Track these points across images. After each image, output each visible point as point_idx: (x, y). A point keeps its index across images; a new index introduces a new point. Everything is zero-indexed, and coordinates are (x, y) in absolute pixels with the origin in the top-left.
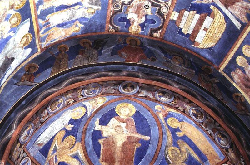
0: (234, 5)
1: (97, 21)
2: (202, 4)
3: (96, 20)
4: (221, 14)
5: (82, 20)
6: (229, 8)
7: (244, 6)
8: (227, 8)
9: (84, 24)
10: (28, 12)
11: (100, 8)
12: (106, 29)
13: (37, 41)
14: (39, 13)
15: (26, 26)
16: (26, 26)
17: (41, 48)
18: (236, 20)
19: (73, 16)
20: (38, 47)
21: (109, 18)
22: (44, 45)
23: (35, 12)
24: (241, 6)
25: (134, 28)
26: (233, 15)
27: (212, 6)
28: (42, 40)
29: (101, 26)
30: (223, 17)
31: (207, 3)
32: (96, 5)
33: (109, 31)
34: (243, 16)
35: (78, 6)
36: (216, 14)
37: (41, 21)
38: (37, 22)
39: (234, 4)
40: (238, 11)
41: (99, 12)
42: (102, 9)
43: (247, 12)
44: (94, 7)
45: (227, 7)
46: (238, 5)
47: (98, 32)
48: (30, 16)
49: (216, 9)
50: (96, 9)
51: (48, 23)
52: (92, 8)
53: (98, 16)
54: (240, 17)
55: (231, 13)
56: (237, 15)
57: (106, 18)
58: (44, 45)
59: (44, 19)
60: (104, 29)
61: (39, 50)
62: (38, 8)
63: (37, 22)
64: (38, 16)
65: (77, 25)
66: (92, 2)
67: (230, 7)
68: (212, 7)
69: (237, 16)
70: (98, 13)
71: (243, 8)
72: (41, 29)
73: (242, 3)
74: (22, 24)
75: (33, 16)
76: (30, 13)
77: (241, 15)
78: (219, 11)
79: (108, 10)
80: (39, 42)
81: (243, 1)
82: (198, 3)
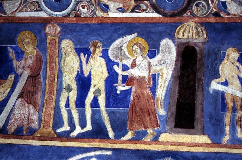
0: (27, 104)
2: (11, 61)
4: (6, 94)
6: (20, 100)
7: (31, 118)
8: (18, 98)
18: (6, 117)
24: (29, 114)
26: (12, 110)
27: (13, 76)
30: (4, 98)
31: (15, 67)
34: (17, 123)
36: (3, 87)
39: (28, 103)
40: (21, 113)
43: (25, 125)
45: (21, 96)
46: (29, 110)
49: (12, 84)
54: (13, 120)
55: (14, 106)
56: (14, 115)
67: (22, 101)
68: (12, 77)
69: (12, 115)
71: (28, 118)
73: (34, 113)
77: (16, 120)
78: (9, 89)
81: (37, 113)
82: (11, 55)
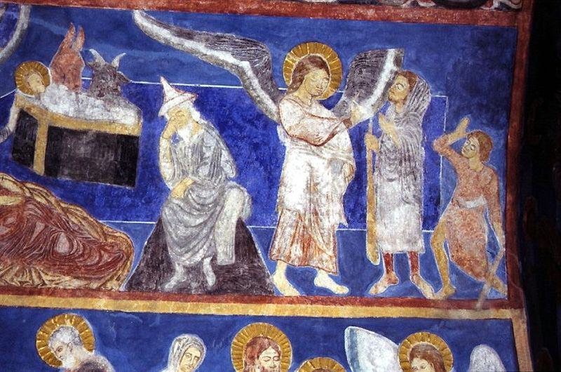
1: (455, 66)
3: (449, 67)
9: (456, 117)
10: (319, 328)
11: (392, 53)
12: (505, 23)
14: (341, 290)
17: (499, 304)
20: (492, 314)
21: (451, 12)
23: (334, 303)
29: (481, 44)
32: (376, 69)
33: (517, 11)
35: (370, 142)
37: (380, 287)
38: (379, 301)
41: (412, 54)
42: (392, 43)
44: (384, 77)
47: (513, 56)
48: (341, 324)
50: (395, 69)
51: (399, 262)
52: (389, 85)
53: (428, 60)
57: (447, 29)
58: (493, 286)
59: (377, 273)
60: (503, 28)
61: (507, 314)
62: (325, 291)
63: (379, 301)
64: (351, 294)
65: (457, 147)
66: (362, 84)
70: (416, 62)
72: (414, 289)
74: (355, 358)
75: (344, 312)
76: (327, 321)
79: (408, 20)
80: (469, 308)
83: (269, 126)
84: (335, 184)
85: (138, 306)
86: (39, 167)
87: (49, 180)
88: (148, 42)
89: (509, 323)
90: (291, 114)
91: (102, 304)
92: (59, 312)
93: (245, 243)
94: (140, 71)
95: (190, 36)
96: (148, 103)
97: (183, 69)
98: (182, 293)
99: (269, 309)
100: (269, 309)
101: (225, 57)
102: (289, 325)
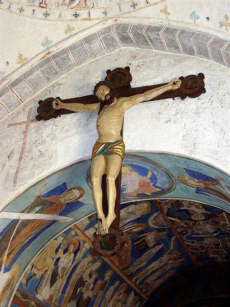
5: (172, 269)
13: (143, 295)
14: (138, 284)
15: (132, 294)
16: (132, 294)
19: (165, 271)
22: (149, 294)
25: (220, 260)
28: (144, 293)
51: (147, 283)
75: (134, 287)
83: (162, 255)
84: (156, 268)
85: (119, 272)
86: (135, 244)
87: (133, 246)
88: (170, 240)
89: (145, 299)
90: (165, 258)
91: (117, 270)
92: (112, 268)
93: (138, 270)
94: (163, 241)
95: (174, 241)
96: (158, 244)
97: (167, 245)
98: (124, 274)
99: (129, 282)
100: (129, 282)
101: (172, 246)
102: (129, 285)
